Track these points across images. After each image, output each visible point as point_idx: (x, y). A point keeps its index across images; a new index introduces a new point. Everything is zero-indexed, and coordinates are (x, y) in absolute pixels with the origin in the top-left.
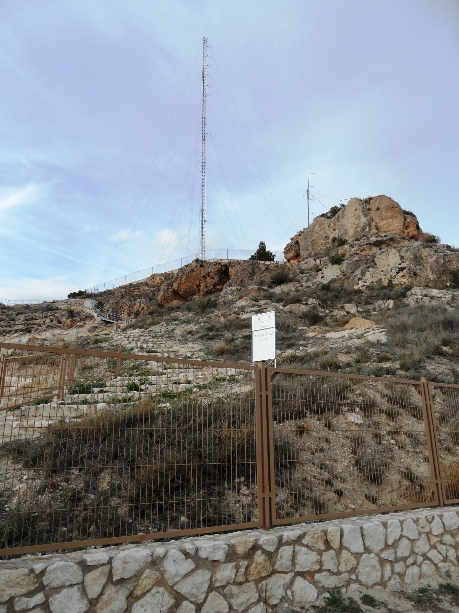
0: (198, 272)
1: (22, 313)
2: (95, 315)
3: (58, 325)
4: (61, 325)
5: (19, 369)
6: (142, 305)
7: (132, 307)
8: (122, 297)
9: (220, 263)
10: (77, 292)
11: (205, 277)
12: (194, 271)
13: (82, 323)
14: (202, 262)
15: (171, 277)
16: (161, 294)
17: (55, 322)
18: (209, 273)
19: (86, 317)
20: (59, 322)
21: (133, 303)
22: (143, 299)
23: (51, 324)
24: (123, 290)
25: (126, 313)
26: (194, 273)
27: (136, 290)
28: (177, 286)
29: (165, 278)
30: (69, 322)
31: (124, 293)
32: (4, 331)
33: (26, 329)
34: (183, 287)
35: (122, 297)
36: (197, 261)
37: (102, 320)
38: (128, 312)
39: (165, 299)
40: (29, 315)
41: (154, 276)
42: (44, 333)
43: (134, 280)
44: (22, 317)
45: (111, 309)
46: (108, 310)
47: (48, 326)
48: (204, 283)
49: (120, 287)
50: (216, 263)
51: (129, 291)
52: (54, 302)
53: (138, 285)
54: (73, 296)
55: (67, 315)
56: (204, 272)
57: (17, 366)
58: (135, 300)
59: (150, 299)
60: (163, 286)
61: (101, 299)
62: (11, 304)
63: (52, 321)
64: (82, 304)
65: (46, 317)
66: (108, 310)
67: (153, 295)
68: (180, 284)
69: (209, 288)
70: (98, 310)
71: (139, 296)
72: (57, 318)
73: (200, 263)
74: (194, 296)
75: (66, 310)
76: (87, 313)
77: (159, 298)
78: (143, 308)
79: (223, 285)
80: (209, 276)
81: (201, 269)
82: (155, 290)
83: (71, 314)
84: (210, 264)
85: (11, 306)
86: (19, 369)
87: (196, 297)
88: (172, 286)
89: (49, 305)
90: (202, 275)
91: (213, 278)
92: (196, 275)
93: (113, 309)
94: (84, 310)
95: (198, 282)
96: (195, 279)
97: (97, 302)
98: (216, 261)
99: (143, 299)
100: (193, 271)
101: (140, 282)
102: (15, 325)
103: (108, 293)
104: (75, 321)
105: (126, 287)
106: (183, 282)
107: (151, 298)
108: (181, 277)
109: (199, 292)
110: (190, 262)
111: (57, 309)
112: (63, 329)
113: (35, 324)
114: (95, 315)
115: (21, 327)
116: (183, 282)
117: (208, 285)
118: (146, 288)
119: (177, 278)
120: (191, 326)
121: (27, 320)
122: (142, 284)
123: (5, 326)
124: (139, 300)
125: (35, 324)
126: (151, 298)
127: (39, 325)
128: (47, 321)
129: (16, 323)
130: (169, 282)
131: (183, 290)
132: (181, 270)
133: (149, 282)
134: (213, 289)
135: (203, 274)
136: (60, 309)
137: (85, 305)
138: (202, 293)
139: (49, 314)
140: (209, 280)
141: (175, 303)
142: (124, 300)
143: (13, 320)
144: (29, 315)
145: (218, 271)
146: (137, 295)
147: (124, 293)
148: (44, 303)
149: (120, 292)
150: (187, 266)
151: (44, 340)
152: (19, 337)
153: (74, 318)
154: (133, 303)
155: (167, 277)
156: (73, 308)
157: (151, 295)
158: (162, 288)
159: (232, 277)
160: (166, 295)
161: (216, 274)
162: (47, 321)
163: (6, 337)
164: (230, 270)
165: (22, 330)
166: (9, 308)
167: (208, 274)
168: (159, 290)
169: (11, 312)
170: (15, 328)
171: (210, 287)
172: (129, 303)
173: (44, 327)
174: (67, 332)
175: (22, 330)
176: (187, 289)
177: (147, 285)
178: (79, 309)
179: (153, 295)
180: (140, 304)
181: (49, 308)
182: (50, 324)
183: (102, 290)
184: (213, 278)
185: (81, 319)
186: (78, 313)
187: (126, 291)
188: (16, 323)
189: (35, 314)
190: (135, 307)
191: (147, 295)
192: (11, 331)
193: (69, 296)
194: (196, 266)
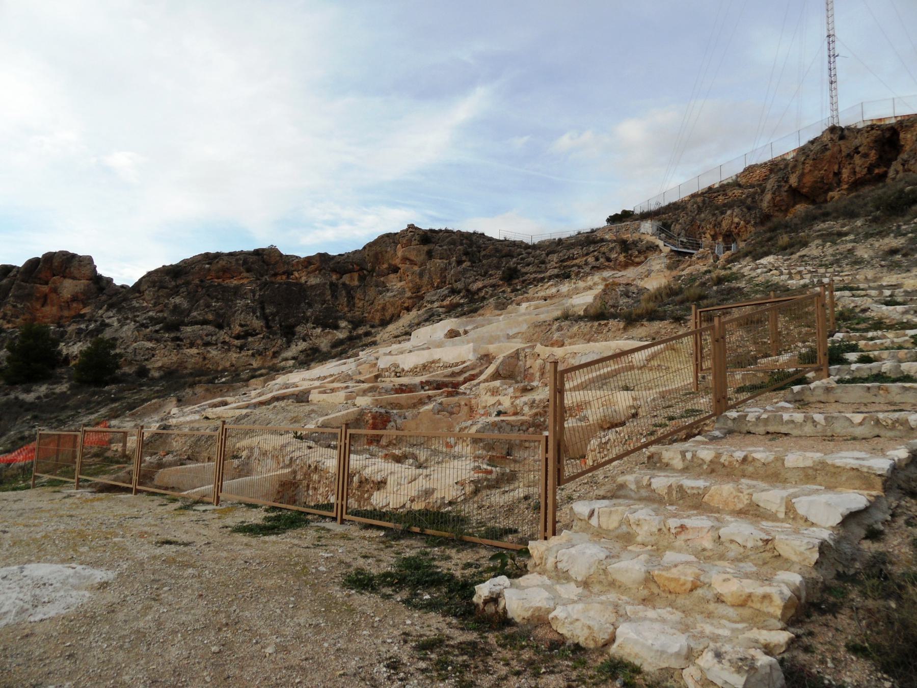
0: (836, 149)
1: (553, 252)
2: (661, 243)
3: (607, 264)
4: (611, 264)
5: (625, 329)
6: (736, 220)
7: (718, 224)
8: (700, 210)
9: (879, 126)
10: (620, 213)
11: (850, 156)
12: (827, 149)
13: (642, 258)
14: (842, 129)
15: (782, 166)
16: (768, 197)
17: (602, 260)
18: (857, 148)
19: (647, 248)
20: (608, 260)
21: (720, 218)
22: (737, 210)
23: (597, 264)
24: (699, 200)
25: (708, 236)
26: (828, 153)
27: (720, 197)
28: (796, 180)
29: (771, 171)
30: (622, 258)
31: (701, 205)
32: (534, 279)
33: (563, 274)
34: (808, 180)
35: (700, 210)
36: (833, 129)
37: (672, 251)
38: (712, 233)
39: (775, 206)
40: (564, 254)
41: (750, 170)
42: (589, 278)
43: (714, 180)
44: (555, 257)
45: (683, 232)
46: (679, 235)
47: (593, 267)
48: (849, 167)
49: (693, 196)
50: (872, 127)
51: (709, 201)
52: (593, 231)
53: (724, 188)
54: (613, 219)
55: (618, 250)
56: (845, 147)
57: (622, 325)
58: (723, 213)
59: (749, 209)
60: (770, 184)
61: (666, 217)
62: (536, 241)
63: (597, 259)
64: (637, 229)
65: (587, 254)
66: (679, 235)
67: (754, 201)
68: (802, 175)
69: (858, 176)
70: (663, 235)
71: (729, 206)
72: (604, 253)
73: (837, 133)
74: (831, 194)
75: (615, 241)
76: (647, 242)
77: (765, 205)
78: (738, 224)
79: (888, 166)
80: (858, 153)
81: (841, 142)
82: (755, 193)
83: (625, 246)
84: (859, 131)
85: (536, 242)
86: (625, 329)
87: (835, 194)
88: (787, 182)
89: (588, 237)
90: (844, 154)
91: (866, 155)
92: (832, 156)
93: (686, 231)
94: (643, 237)
95: (836, 167)
96: (829, 162)
97: (660, 223)
98: (869, 123)
99: (737, 210)
100: (825, 148)
101: (725, 182)
102: (546, 270)
103: (674, 208)
104: (631, 256)
105: (703, 193)
106: (806, 171)
107: (749, 205)
108: (804, 163)
109: (839, 183)
110: (819, 134)
111: (602, 240)
112: (613, 269)
113: (573, 266)
114: (661, 243)
115: (556, 271)
116: (806, 171)
117: (858, 169)
118: (738, 192)
119: (795, 166)
120: (887, 240)
121: (562, 261)
122: (728, 184)
123: (535, 272)
124: (729, 212)
125: (573, 266)
126: (749, 205)
127: (579, 267)
128: (591, 259)
129: (548, 266)
130: (780, 174)
131: (808, 184)
132: (802, 150)
133: (743, 181)
134: (868, 176)
135: (845, 151)
136: (606, 241)
137: (642, 230)
138: (846, 186)
139: (591, 249)
140: (857, 160)
141: (801, 208)
142: (703, 215)
143: (543, 262)
144: (564, 254)
145: (875, 141)
146: (724, 205)
147: (701, 205)
148: (579, 233)
149: (696, 203)
150: (812, 142)
151: (628, 284)
152: (555, 285)
153: (630, 252)
154: (720, 218)
155: (776, 167)
156: (625, 237)
157: (749, 200)
158: (769, 187)
159: (907, 148)
160: (778, 198)
161: (871, 148)
162: (591, 259)
163: (539, 287)
164: (902, 135)
165: (557, 276)
166: (534, 247)
167: (856, 150)
168: (763, 191)
169: (538, 252)
170: (548, 274)
171: (861, 172)
172: (712, 219)
173: (587, 269)
174: (620, 274)
175: (557, 276)
176: (816, 182)
177: (740, 186)
178: (636, 236)
179: (754, 201)
180: (732, 218)
181: (588, 241)
182: (594, 264)
183: (665, 203)
184: (866, 155)
185: (640, 252)
186: (635, 243)
187: (704, 200)
188: (548, 266)
189: (571, 251)
190: (724, 224)
191: (742, 202)
192: (542, 279)
193: (608, 220)
194: (832, 139)
